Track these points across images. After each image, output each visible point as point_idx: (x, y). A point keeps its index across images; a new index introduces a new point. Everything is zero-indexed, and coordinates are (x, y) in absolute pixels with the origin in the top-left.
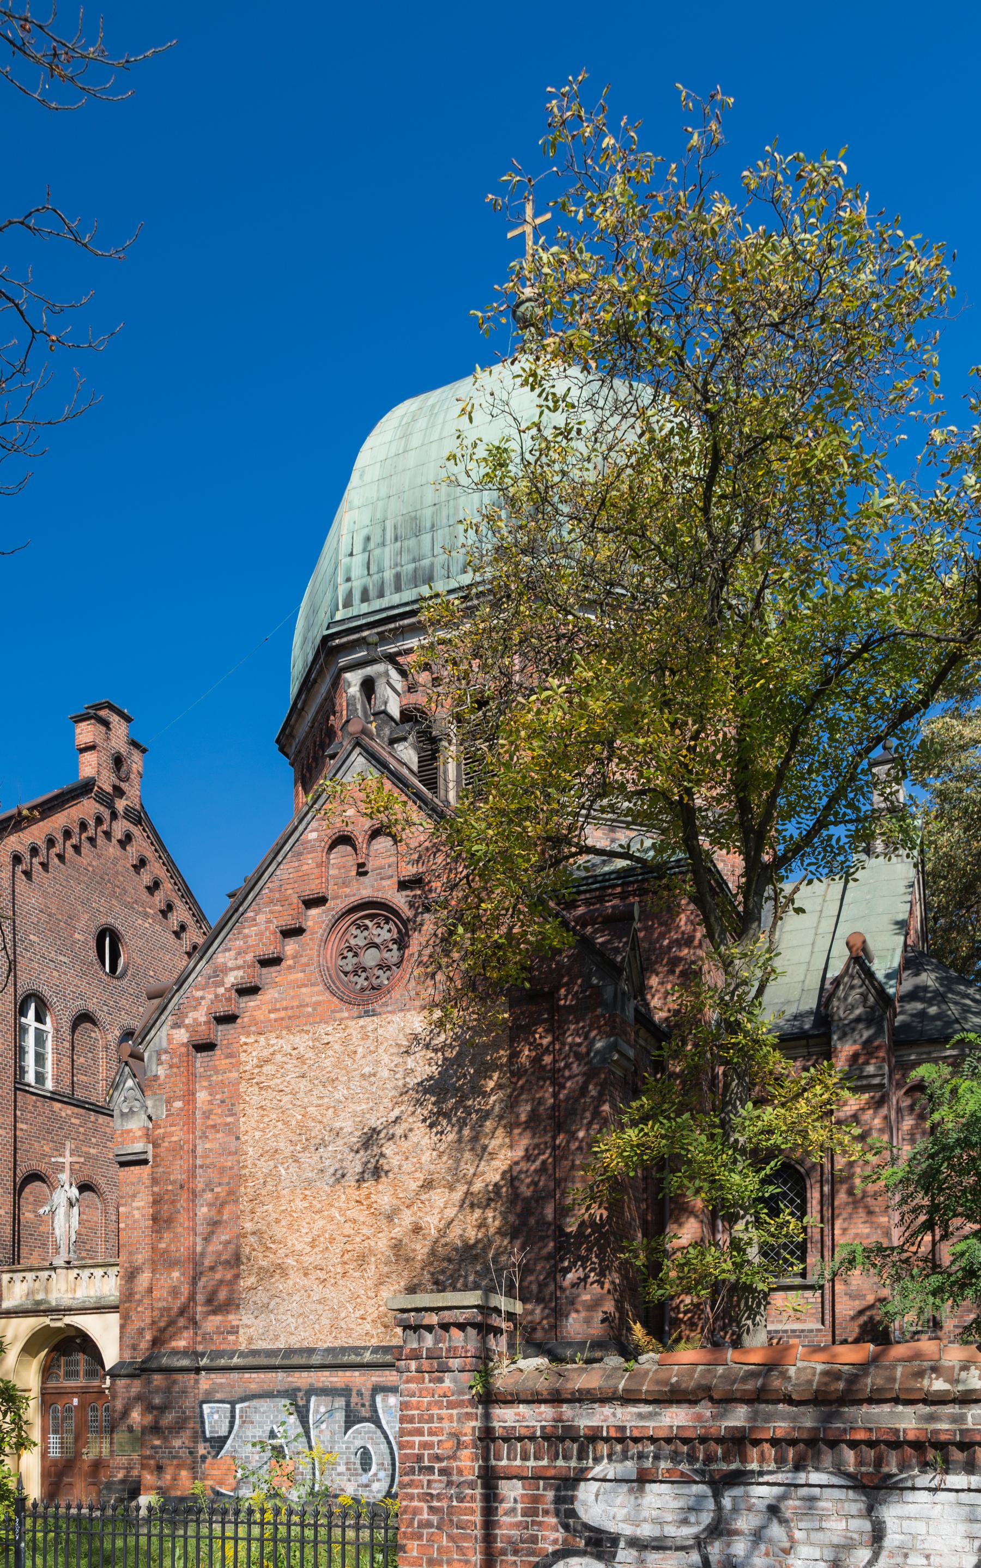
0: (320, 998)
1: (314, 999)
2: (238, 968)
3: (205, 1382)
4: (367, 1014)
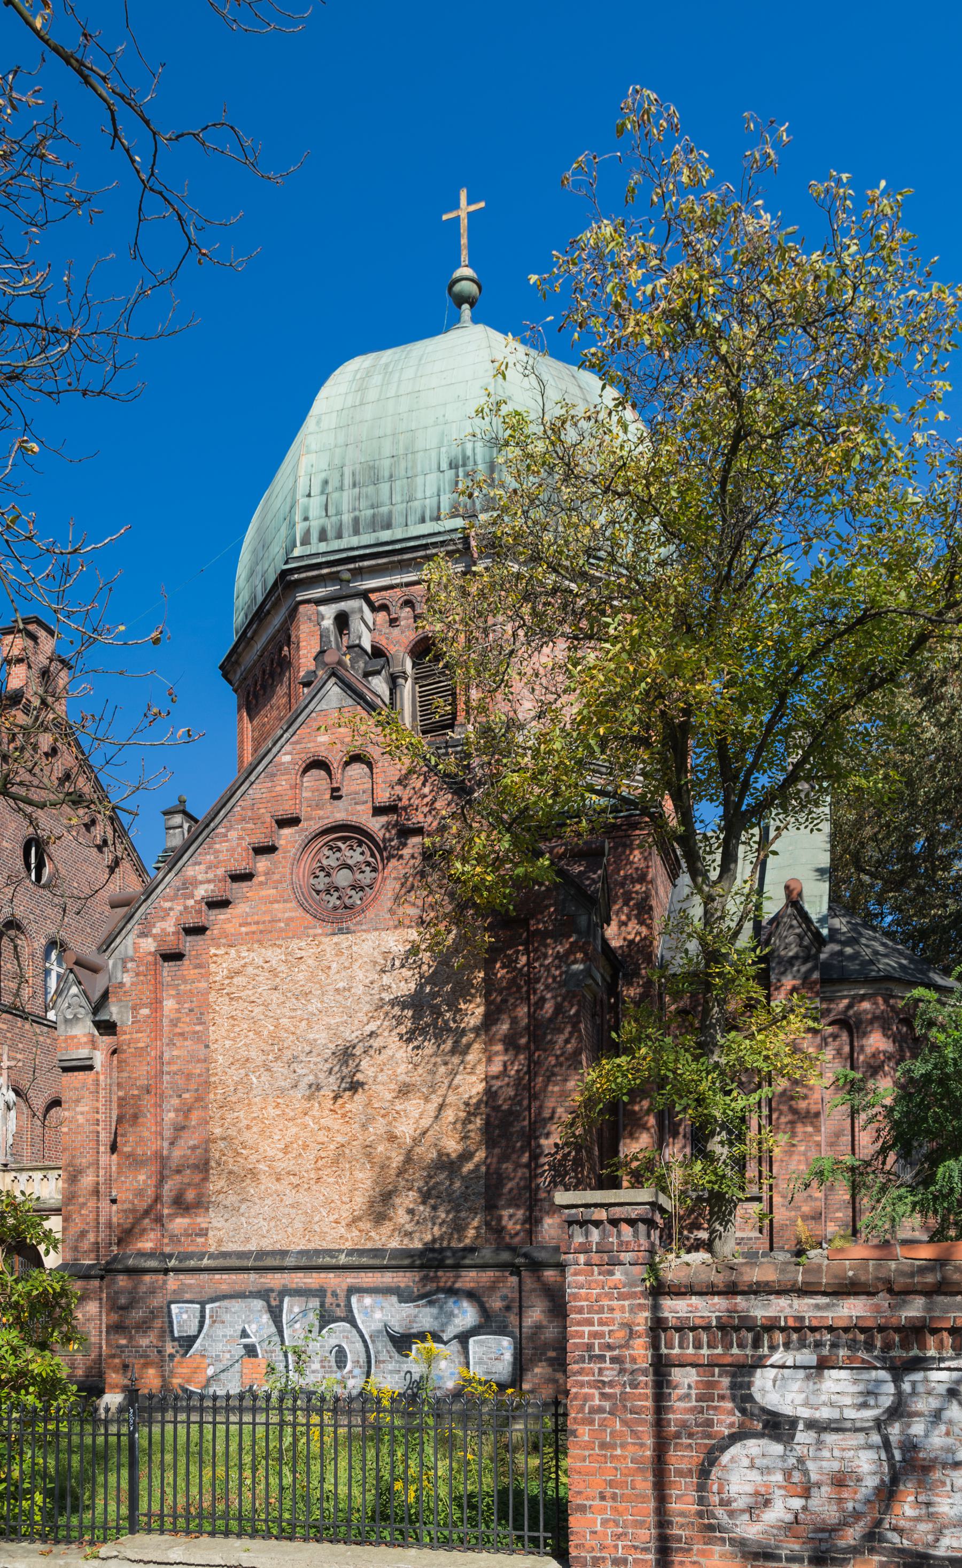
0: (293, 914)
1: (287, 915)
2: (209, 881)
3: (172, 1282)
4: (341, 931)
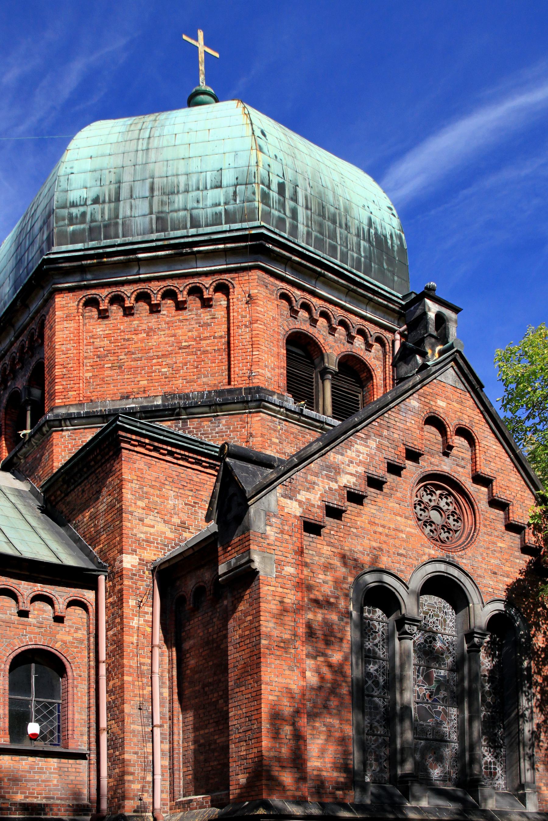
0: (413, 531)
1: (408, 529)
2: (351, 474)
